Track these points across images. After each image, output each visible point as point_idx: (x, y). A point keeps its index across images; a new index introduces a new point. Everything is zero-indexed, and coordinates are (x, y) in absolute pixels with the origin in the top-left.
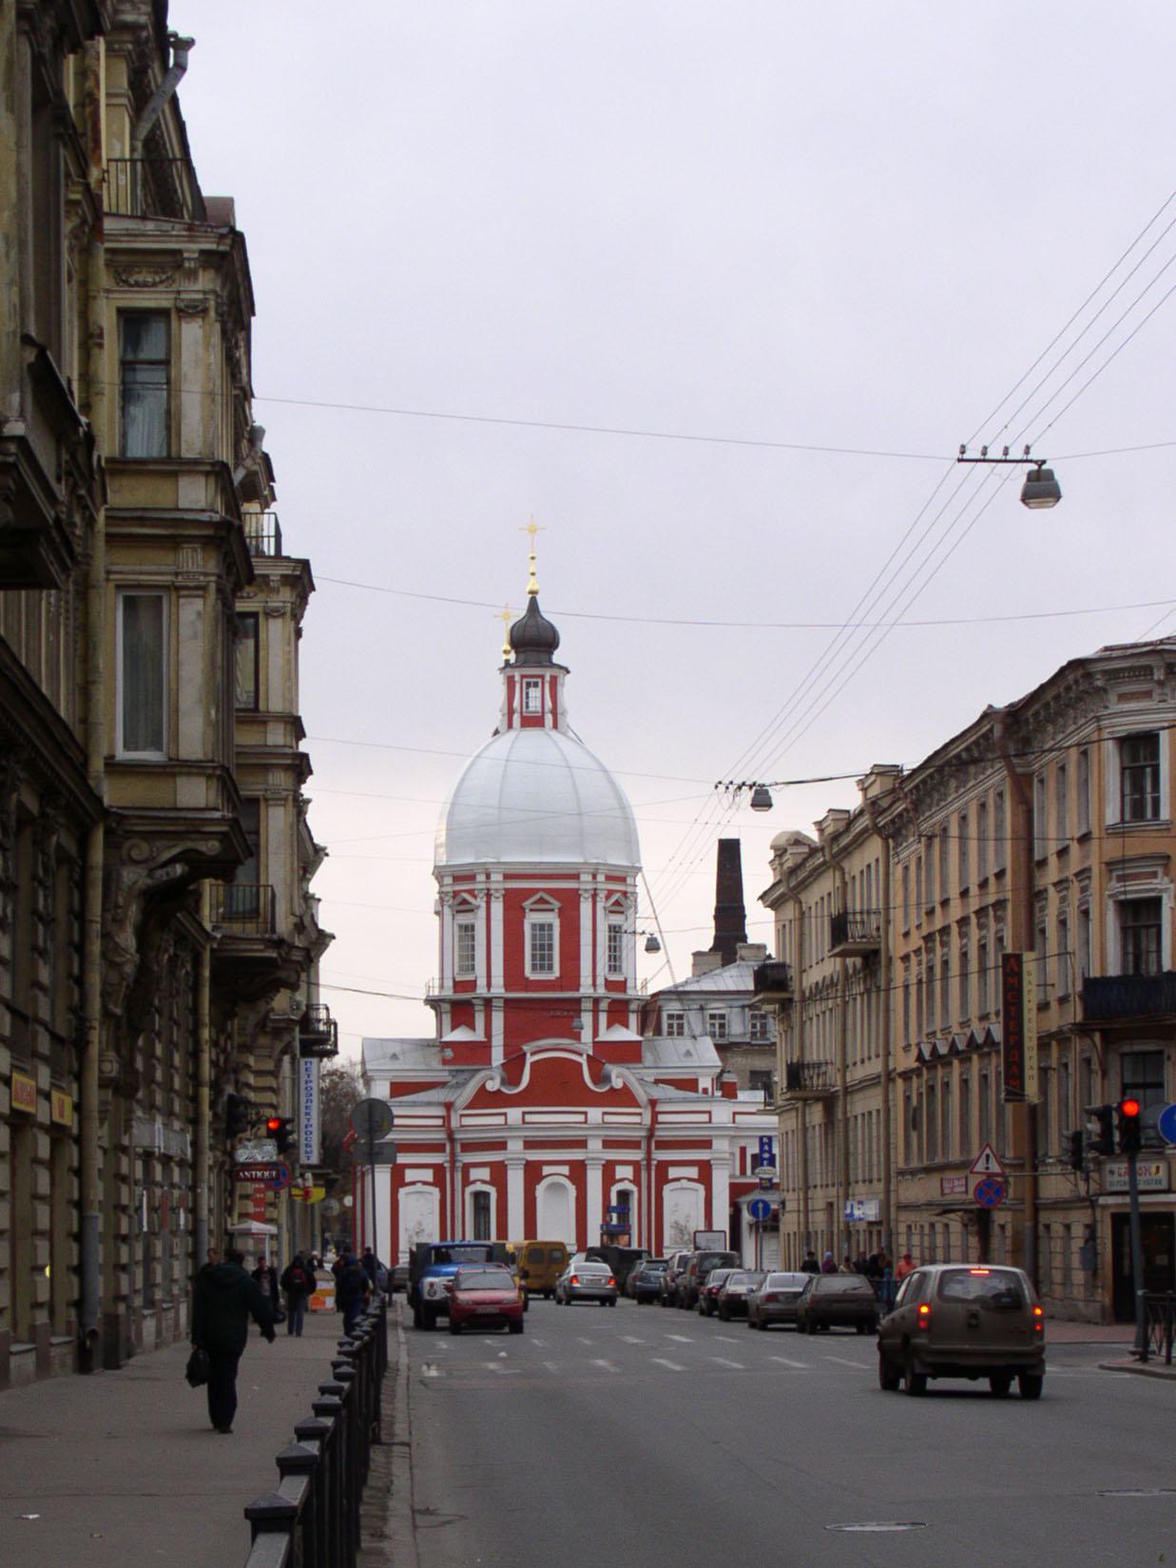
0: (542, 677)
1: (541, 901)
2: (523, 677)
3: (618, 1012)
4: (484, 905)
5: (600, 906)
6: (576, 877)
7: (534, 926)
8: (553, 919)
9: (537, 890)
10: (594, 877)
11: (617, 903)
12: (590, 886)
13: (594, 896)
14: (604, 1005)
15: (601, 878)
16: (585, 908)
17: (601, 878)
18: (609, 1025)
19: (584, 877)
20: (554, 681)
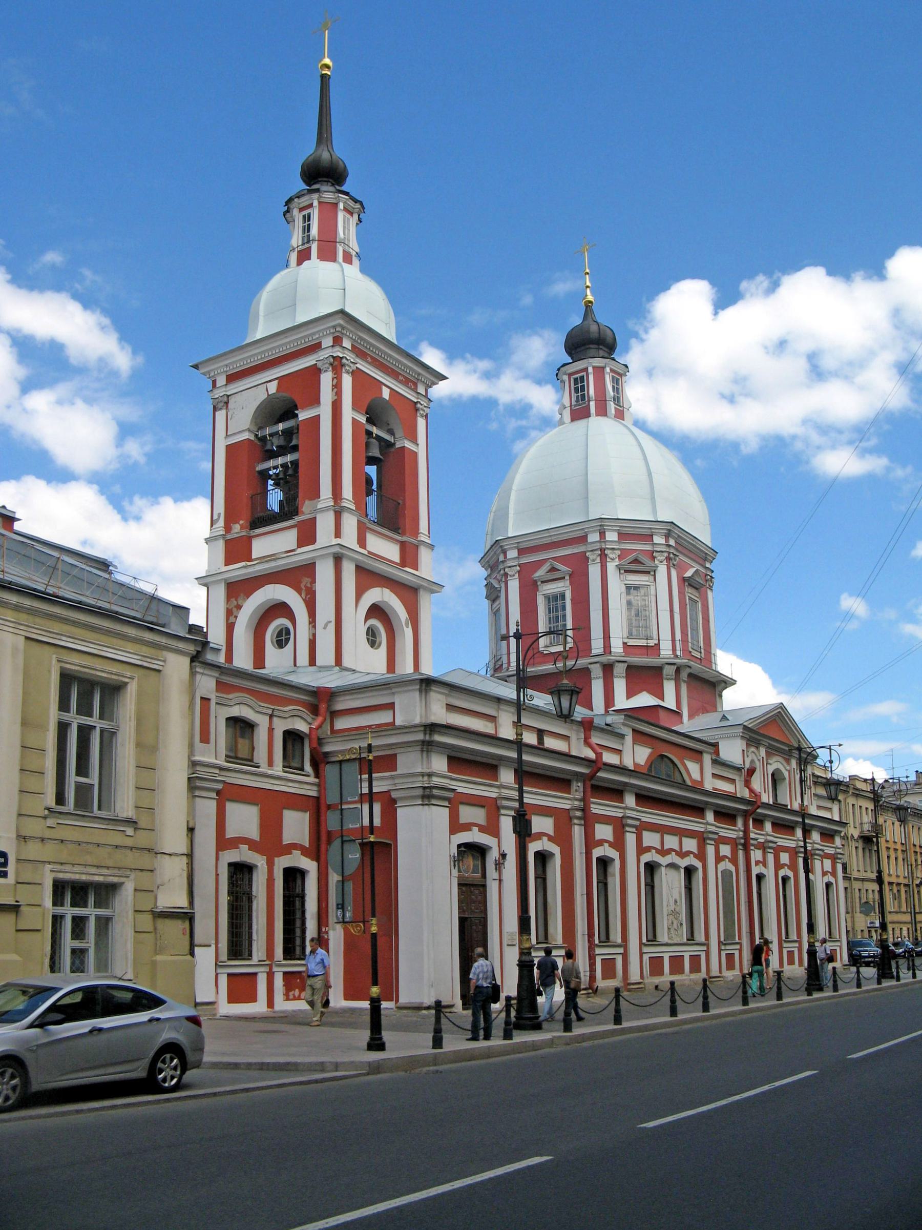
0: (586, 370)
1: (553, 569)
2: (570, 375)
3: (645, 676)
4: (503, 585)
5: (611, 567)
6: (583, 539)
7: (548, 598)
8: (564, 587)
9: (545, 561)
10: (602, 534)
11: (636, 561)
12: (598, 546)
13: (603, 556)
14: (620, 669)
15: (611, 536)
16: (594, 571)
17: (611, 536)
18: (630, 694)
19: (590, 540)
20: (599, 371)
